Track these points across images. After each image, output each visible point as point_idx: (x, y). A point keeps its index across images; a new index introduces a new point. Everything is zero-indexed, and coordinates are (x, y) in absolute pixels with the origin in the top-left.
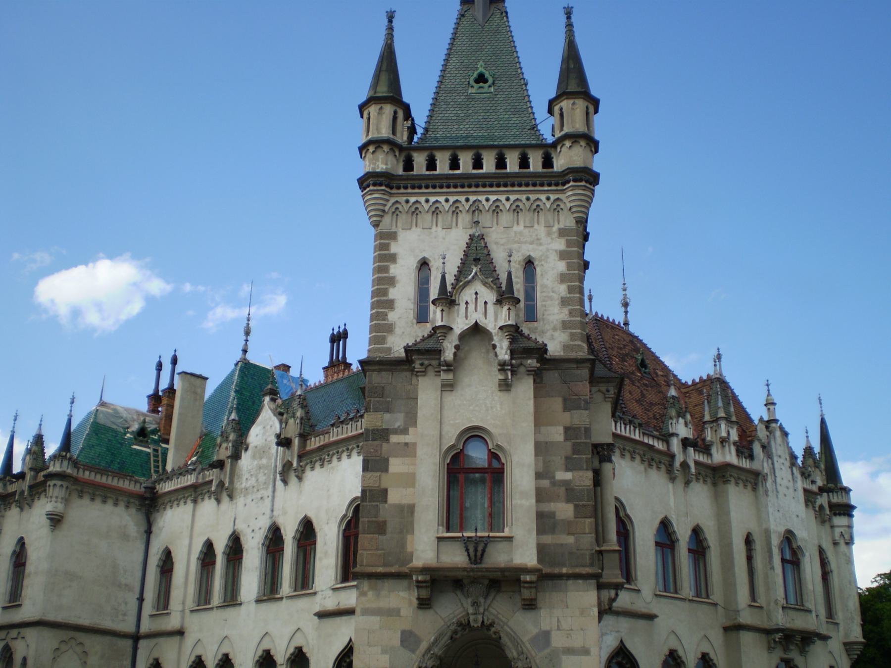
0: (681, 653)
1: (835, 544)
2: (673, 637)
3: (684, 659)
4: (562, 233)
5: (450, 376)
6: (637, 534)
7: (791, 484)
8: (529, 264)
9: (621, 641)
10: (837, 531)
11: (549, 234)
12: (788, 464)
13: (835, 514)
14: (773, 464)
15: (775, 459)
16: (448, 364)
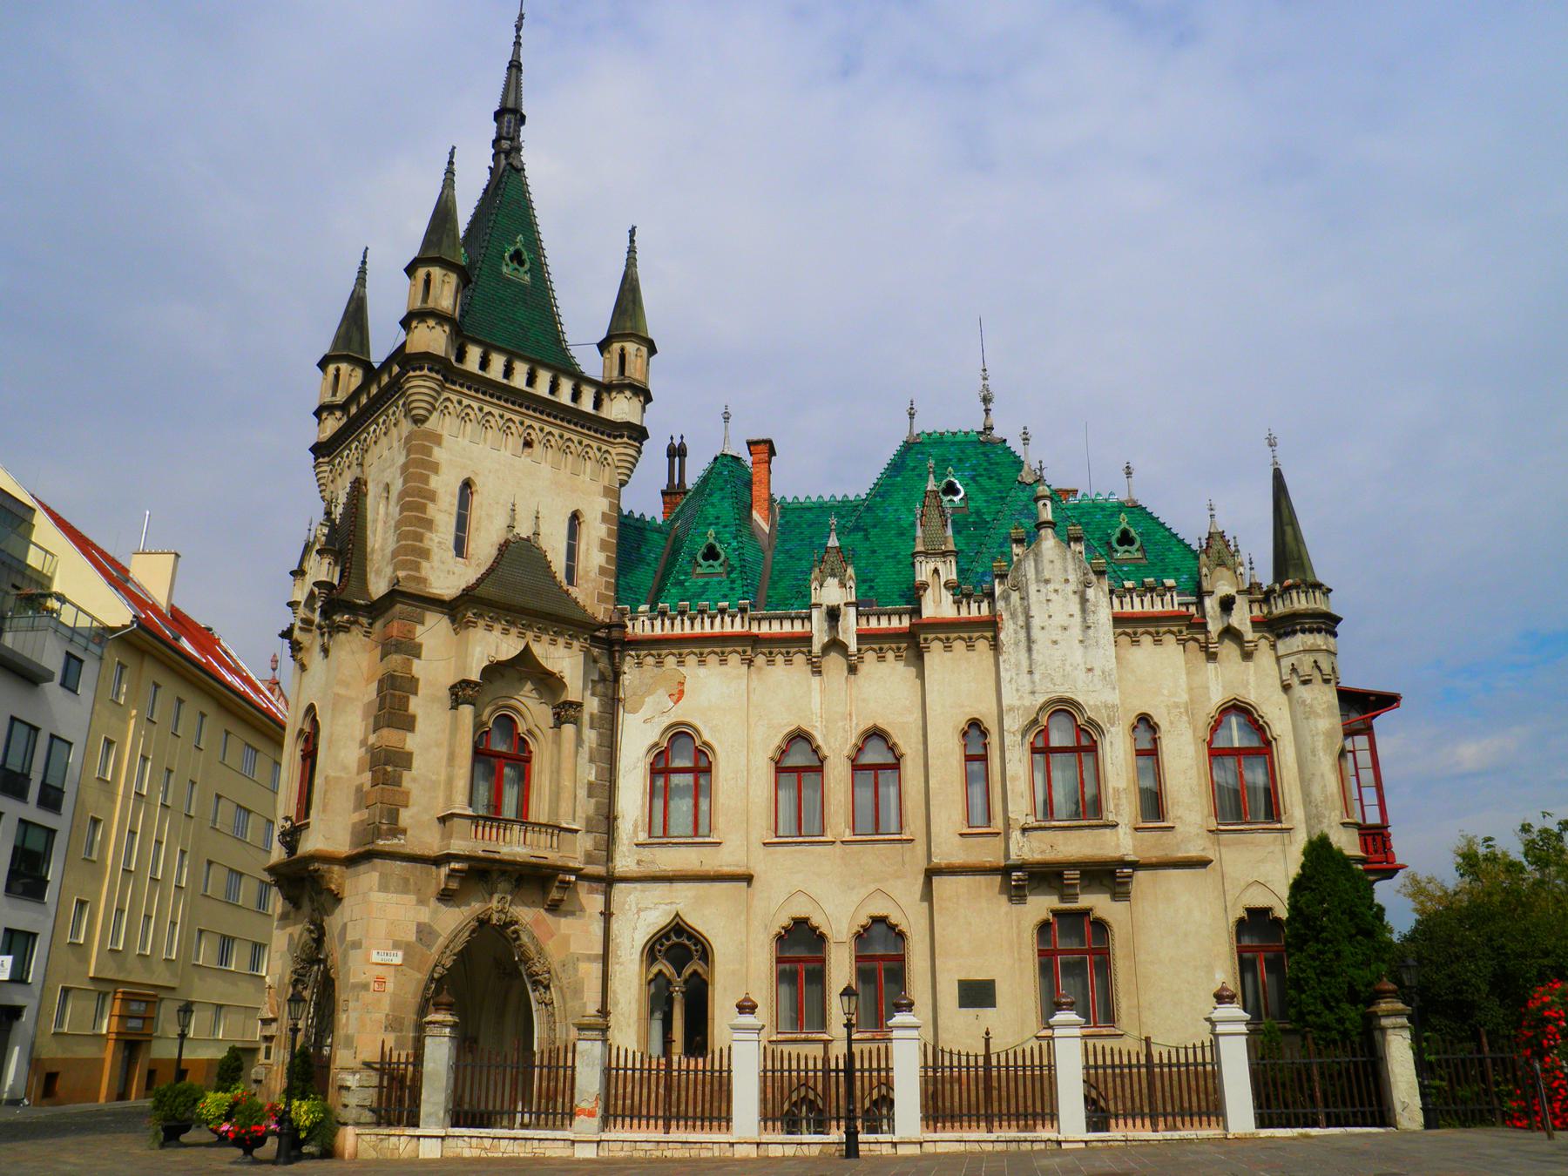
0: (816, 920)
1: (1286, 688)
2: (803, 898)
3: (824, 929)
9: (677, 915)
12: (1072, 586)
13: (1279, 636)
15: (1033, 588)
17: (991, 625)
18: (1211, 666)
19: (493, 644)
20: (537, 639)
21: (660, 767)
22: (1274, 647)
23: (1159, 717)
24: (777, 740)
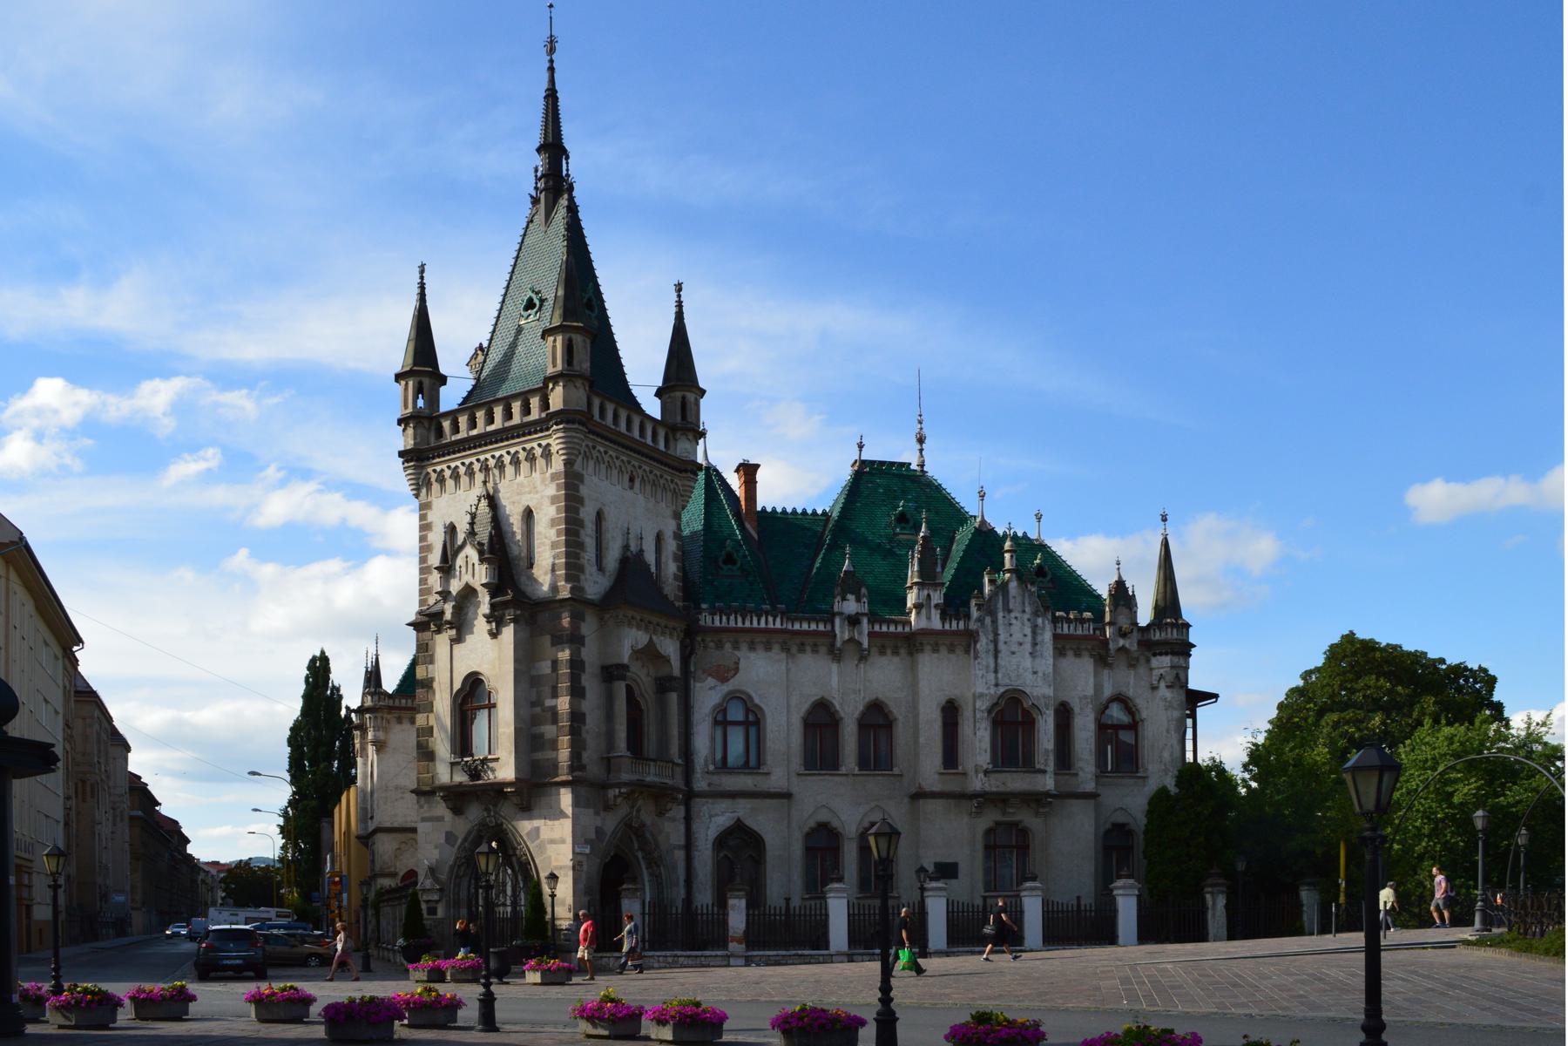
4: (554, 477)
5: (453, 632)
6: (769, 720)
7: (1029, 638)
8: (528, 514)
10: (1156, 673)
11: (543, 481)
12: (1026, 616)
14: (994, 622)
15: (1000, 615)
16: (448, 622)
17: (970, 637)
18: (1106, 672)
21: (721, 721)
22: (1148, 661)
23: (1076, 706)
24: (806, 707)
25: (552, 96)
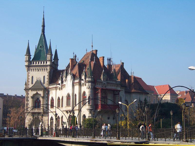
19: (35, 92)
20: (38, 91)
25: (44, 19)
